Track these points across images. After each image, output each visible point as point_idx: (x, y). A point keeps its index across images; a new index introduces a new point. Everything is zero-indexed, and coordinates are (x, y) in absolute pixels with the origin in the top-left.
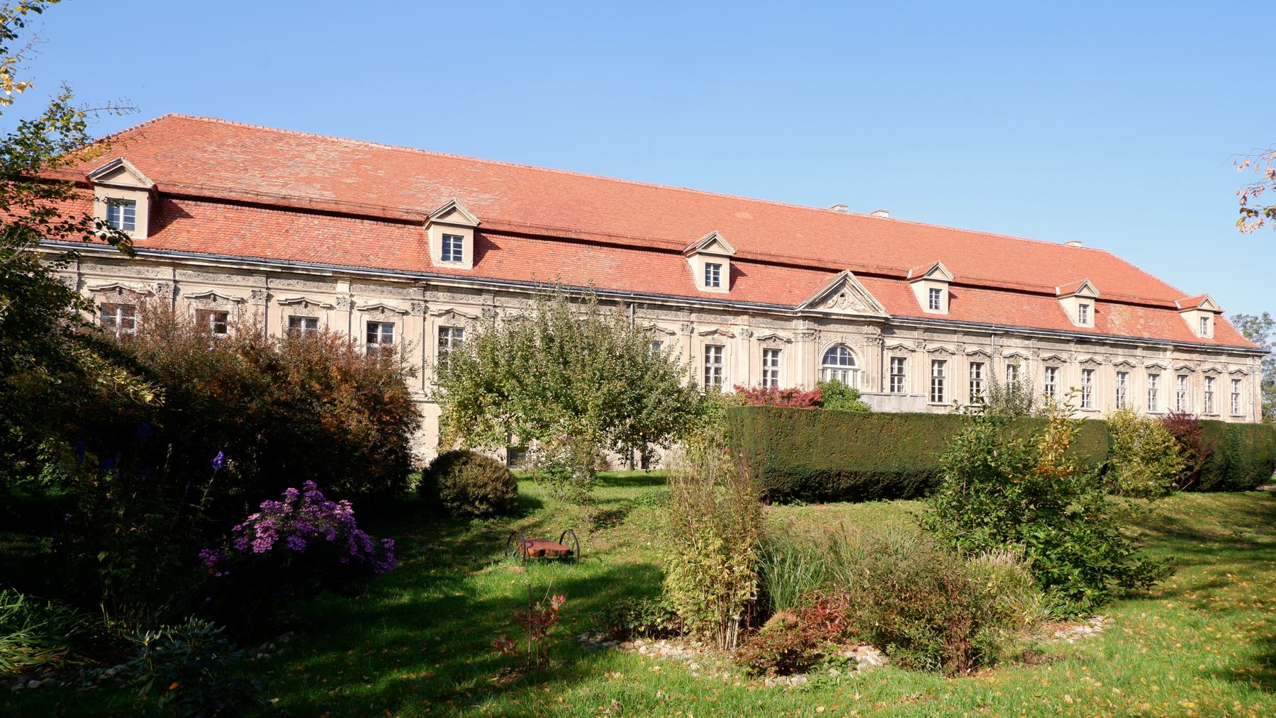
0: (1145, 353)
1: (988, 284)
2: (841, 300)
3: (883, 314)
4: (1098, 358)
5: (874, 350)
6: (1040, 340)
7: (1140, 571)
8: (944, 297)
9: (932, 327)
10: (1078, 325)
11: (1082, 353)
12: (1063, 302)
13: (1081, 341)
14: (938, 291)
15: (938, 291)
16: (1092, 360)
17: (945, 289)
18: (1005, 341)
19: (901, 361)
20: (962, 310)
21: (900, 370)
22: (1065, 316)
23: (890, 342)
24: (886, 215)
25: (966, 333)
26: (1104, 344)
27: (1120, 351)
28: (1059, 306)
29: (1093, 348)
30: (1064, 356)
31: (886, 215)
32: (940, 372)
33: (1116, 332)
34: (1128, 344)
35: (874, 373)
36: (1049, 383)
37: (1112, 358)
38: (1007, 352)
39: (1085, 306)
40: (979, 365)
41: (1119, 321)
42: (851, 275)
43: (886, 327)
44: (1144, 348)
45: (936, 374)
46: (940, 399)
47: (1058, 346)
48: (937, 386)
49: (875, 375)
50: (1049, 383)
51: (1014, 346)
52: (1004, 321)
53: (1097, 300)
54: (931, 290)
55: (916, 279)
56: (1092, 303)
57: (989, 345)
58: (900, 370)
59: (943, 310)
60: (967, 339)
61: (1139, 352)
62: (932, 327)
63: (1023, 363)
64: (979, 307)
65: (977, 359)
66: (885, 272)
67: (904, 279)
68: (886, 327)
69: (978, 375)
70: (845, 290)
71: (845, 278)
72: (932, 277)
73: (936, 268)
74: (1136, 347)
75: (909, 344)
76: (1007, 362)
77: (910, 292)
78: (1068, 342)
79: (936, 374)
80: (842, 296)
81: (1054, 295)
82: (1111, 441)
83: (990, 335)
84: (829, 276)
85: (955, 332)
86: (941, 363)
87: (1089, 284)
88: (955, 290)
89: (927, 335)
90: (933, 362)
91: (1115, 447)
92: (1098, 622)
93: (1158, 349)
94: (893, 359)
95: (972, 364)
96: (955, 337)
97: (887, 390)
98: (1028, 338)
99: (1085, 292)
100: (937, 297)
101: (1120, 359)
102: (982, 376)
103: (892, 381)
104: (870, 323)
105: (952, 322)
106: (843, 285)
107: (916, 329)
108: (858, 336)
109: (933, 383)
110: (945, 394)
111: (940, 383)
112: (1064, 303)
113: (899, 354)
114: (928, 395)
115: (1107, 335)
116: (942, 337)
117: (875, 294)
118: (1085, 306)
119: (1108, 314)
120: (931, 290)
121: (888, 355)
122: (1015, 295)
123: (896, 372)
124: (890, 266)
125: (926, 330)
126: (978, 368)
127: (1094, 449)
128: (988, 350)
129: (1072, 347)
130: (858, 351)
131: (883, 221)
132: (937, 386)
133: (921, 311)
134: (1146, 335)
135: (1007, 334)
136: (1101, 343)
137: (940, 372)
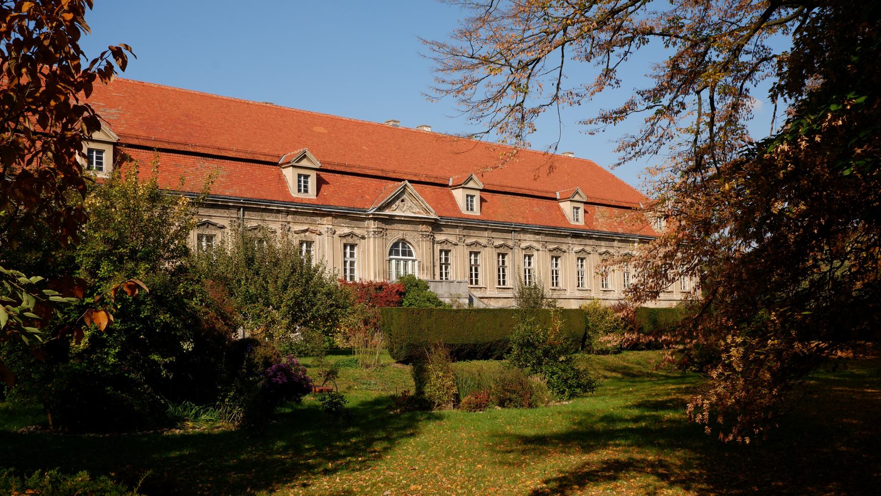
0: (620, 244)
1: (508, 190)
2: (401, 204)
3: (433, 216)
4: (588, 249)
5: (426, 245)
6: (547, 235)
7: (588, 384)
8: (476, 202)
9: (468, 225)
10: (573, 223)
11: (576, 246)
12: (562, 205)
13: (576, 236)
14: (472, 197)
15: (472, 197)
16: (583, 250)
17: (477, 194)
18: (522, 236)
19: (447, 252)
20: (490, 211)
21: (446, 259)
22: (564, 216)
23: (439, 237)
24: (429, 129)
25: (494, 230)
26: (592, 238)
27: (603, 243)
28: (559, 207)
29: (584, 241)
30: (564, 247)
31: (429, 129)
32: (476, 261)
33: (599, 228)
34: (608, 238)
35: (427, 263)
36: (554, 268)
37: (597, 248)
38: (524, 245)
39: (578, 208)
40: (504, 255)
41: (603, 220)
42: (409, 184)
43: (436, 225)
44: (620, 241)
45: (473, 262)
46: (477, 282)
47: (559, 240)
48: (474, 272)
49: (429, 264)
50: (554, 268)
51: (528, 240)
52: (521, 220)
53: (585, 203)
54: (467, 196)
55: (455, 187)
56: (582, 206)
57: (510, 239)
58: (446, 259)
59: (476, 212)
60: (494, 235)
61: (616, 244)
62: (468, 225)
63: (535, 253)
64: (504, 209)
65: (502, 250)
66: (432, 180)
67: (447, 186)
68: (436, 225)
69: (503, 262)
70: (405, 196)
71: (405, 187)
72: (467, 186)
73: (471, 179)
74: (614, 240)
75: (452, 239)
76: (524, 252)
77: (452, 197)
78: (566, 236)
79: (473, 262)
80: (403, 201)
81: (555, 199)
82: (587, 321)
83: (511, 232)
84: (391, 184)
85: (486, 229)
86: (476, 254)
87: (580, 191)
88: (486, 195)
89: (465, 232)
90: (471, 253)
91: (590, 324)
92: (571, 402)
93: (629, 242)
94: (441, 251)
95: (499, 254)
96: (486, 234)
97: (437, 278)
98: (538, 234)
99: (577, 198)
100: (472, 201)
101: (603, 250)
102: (506, 264)
103: (441, 269)
104: (423, 223)
105: (483, 221)
106: (403, 192)
107: (457, 227)
108: (415, 233)
109: (471, 270)
110: (480, 278)
111: (476, 270)
112: (562, 205)
113: (445, 247)
114: (467, 279)
115: (594, 231)
116: (477, 233)
117: (426, 199)
118: (578, 208)
119: (594, 214)
120: (467, 196)
121: (438, 248)
122: (527, 199)
123: (443, 261)
124: (435, 175)
125: (465, 228)
126: (503, 258)
127: (578, 327)
128: (510, 243)
129: (569, 240)
130: (417, 247)
131: (426, 134)
132: (474, 272)
133: (460, 212)
134: (620, 231)
135: (524, 231)
136: (589, 237)
137: (476, 261)
